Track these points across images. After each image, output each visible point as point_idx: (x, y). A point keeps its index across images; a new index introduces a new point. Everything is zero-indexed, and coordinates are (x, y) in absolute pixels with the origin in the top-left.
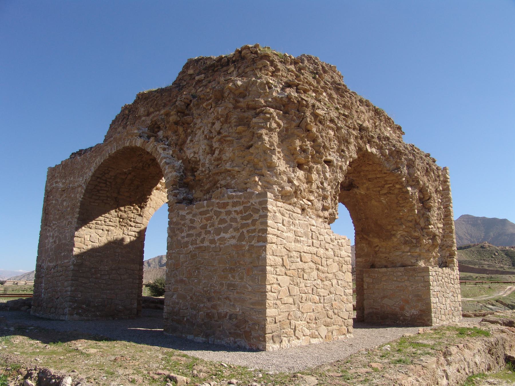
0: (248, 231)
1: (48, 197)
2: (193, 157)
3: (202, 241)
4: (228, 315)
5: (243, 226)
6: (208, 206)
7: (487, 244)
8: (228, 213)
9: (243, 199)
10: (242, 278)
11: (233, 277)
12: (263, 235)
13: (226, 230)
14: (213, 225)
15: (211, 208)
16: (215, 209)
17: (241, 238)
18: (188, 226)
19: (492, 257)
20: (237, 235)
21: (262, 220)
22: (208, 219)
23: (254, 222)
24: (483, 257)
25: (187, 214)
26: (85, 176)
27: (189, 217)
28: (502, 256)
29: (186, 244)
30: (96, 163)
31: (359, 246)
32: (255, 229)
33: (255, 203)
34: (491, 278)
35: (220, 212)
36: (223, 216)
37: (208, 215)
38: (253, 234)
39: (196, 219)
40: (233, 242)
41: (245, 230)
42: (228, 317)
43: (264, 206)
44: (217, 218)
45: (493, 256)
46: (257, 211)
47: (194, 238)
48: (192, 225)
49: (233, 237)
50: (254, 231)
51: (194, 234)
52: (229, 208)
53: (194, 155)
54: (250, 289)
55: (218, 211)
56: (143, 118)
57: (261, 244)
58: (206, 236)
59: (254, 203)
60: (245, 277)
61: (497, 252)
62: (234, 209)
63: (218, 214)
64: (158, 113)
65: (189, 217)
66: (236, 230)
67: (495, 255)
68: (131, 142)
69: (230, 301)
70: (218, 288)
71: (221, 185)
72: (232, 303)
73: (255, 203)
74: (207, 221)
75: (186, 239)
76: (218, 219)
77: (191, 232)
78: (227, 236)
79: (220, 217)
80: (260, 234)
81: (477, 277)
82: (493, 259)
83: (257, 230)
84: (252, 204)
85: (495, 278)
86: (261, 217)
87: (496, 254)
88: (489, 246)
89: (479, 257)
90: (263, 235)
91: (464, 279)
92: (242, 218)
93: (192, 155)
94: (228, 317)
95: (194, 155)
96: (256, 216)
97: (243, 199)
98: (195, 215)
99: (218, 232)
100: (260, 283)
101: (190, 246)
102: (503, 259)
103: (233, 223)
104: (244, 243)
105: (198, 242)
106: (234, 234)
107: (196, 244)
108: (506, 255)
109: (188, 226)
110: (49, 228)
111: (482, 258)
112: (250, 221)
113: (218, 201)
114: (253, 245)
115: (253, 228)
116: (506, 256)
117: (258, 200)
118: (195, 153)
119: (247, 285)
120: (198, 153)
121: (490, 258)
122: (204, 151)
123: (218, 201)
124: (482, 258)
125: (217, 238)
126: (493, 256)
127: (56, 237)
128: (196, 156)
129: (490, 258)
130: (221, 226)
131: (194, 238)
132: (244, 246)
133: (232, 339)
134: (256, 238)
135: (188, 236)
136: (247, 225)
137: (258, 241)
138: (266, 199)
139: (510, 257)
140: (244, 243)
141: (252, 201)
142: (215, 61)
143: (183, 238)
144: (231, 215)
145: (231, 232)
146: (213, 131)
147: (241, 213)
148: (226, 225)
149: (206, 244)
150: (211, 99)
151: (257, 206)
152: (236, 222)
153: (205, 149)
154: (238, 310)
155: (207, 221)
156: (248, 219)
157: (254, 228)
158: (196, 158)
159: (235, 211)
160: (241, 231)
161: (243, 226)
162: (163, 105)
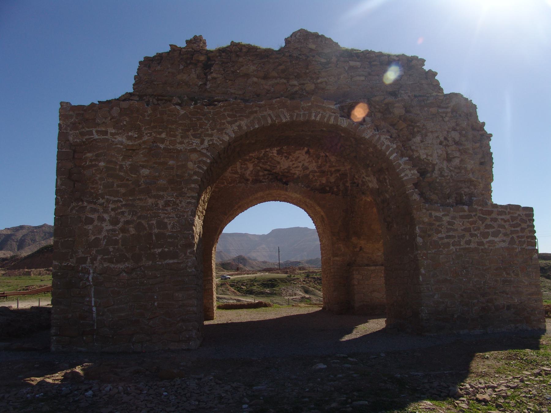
0: (518, 237)
1: (75, 151)
2: (425, 158)
3: (468, 242)
4: (506, 306)
5: (512, 232)
6: (469, 211)
8: (495, 220)
9: (508, 210)
10: (517, 275)
11: (508, 274)
12: (532, 241)
13: (495, 234)
14: (479, 229)
15: (474, 214)
16: (478, 214)
17: (512, 241)
18: (447, 228)
20: (508, 239)
21: (529, 229)
22: (472, 223)
23: (523, 230)
25: (443, 215)
26: (207, 139)
27: (446, 219)
29: (447, 245)
30: (240, 127)
31: (336, 246)
32: (524, 236)
33: (523, 215)
35: (486, 219)
36: (488, 222)
37: (471, 219)
38: (523, 240)
39: (456, 222)
40: (503, 245)
41: (515, 236)
42: (505, 308)
43: (530, 218)
44: (483, 223)
46: (525, 222)
47: (456, 239)
48: (449, 227)
49: (504, 241)
50: (522, 237)
51: (456, 236)
52: (494, 216)
53: (427, 157)
54: (526, 283)
55: (482, 217)
56: (255, 79)
57: (530, 247)
58: (472, 239)
59: (521, 215)
60: (520, 274)
62: (500, 217)
63: (483, 220)
64: (285, 81)
65: (446, 219)
66: (505, 235)
68: (323, 117)
69: (507, 294)
70: (492, 285)
71: (465, 192)
72: (509, 296)
73: (523, 215)
74: (471, 224)
75: (445, 240)
76: (484, 225)
77: (450, 234)
78: (496, 239)
79: (486, 223)
80: (529, 240)
83: (525, 237)
84: (519, 215)
86: (528, 226)
90: (532, 241)
92: (512, 226)
93: (425, 156)
94: (505, 308)
95: (427, 157)
96: (524, 225)
97: (508, 210)
98: (454, 218)
99: (485, 235)
100: (534, 278)
101: (452, 247)
103: (501, 229)
104: (515, 246)
105: (462, 243)
106: (505, 238)
107: (460, 245)
109: (447, 228)
110: (93, 206)
112: (519, 229)
113: (480, 208)
114: (524, 248)
115: (521, 234)
117: (524, 213)
118: (427, 155)
119: (523, 280)
120: (431, 156)
122: (440, 156)
123: (480, 208)
125: (485, 241)
127: (127, 223)
128: (429, 158)
130: (488, 230)
131: (456, 239)
132: (516, 248)
133: (513, 325)
134: (526, 243)
135: (448, 237)
136: (517, 232)
137: (528, 246)
138: (532, 213)
140: (515, 246)
141: (520, 213)
142: (374, 55)
143: (442, 238)
144: (497, 222)
145: (501, 237)
146: (450, 139)
147: (508, 221)
148: (493, 230)
149: (472, 246)
150: (447, 108)
151: (524, 218)
152: (505, 228)
153: (441, 154)
154: (516, 301)
155: (471, 224)
156: (517, 227)
157: (523, 234)
158: (429, 160)
159: (502, 219)
160: (511, 236)
161: (512, 232)
162: (296, 74)
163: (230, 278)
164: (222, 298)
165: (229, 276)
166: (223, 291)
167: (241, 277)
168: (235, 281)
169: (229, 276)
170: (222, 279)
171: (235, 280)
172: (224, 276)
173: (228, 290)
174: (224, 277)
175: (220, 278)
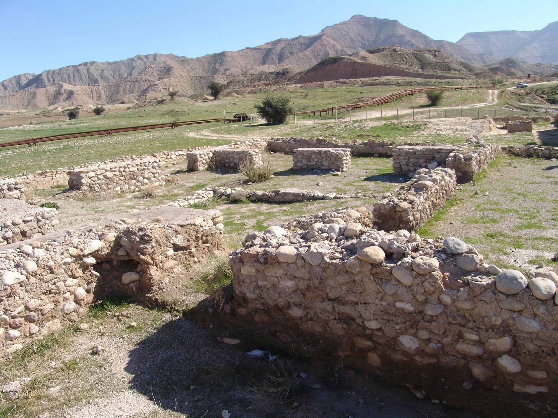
7: (398, 48)
19: (404, 61)
24: (395, 61)
28: (412, 59)
34: (449, 82)
45: (405, 60)
61: (408, 56)
67: (406, 58)
81: (435, 82)
82: (404, 63)
85: (452, 83)
87: (407, 57)
88: (401, 50)
89: (392, 60)
91: (423, 84)
102: (413, 63)
108: (416, 58)
111: (395, 62)
116: (415, 60)
121: (402, 62)
124: (395, 62)
126: (405, 60)
129: (402, 62)
139: (419, 60)
163: (527, 86)
164: (540, 108)
165: (526, 85)
166: (530, 100)
167: (540, 85)
168: (535, 90)
169: (526, 85)
170: (518, 88)
171: (533, 88)
172: (520, 84)
173: (536, 99)
174: (521, 86)
175: (514, 86)
